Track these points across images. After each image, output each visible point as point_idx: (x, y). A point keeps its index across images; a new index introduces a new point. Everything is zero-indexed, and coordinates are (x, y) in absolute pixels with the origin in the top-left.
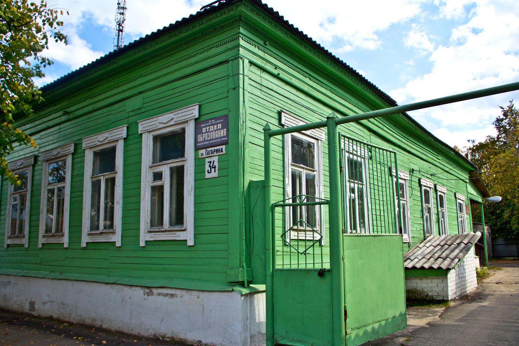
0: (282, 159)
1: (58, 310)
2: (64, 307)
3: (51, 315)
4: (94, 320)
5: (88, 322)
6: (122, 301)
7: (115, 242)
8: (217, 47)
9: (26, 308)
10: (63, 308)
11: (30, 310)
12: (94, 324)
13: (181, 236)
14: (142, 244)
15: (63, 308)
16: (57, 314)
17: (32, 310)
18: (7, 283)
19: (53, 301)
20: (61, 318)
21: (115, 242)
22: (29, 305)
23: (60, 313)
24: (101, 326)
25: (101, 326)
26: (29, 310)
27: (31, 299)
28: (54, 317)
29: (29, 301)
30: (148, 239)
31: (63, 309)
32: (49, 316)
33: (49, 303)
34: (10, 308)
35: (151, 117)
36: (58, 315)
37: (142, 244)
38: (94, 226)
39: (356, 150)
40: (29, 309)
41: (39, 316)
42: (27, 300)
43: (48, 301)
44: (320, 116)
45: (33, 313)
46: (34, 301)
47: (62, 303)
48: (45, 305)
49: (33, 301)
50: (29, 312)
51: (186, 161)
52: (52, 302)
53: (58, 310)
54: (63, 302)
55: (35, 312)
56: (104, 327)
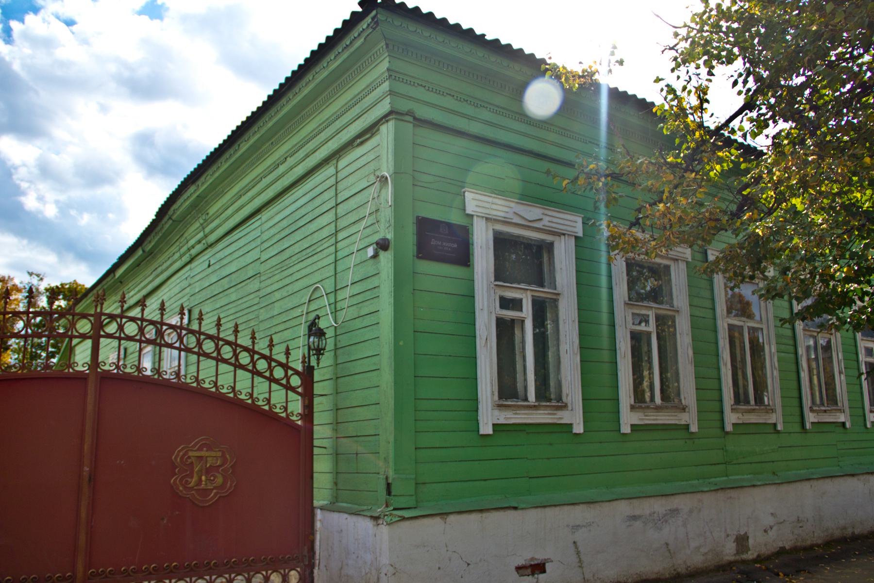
0: (853, 344)
1: (793, 533)
2: (801, 525)
3: (782, 546)
4: (844, 528)
5: (838, 534)
6: (870, 493)
7: (571, 425)
8: (406, 83)
9: (729, 551)
10: (801, 527)
11: (738, 553)
12: (845, 535)
13: (683, 418)
14: (626, 429)
15: (801, 527)
16: (791, 540)
17: (742, 553)
18: (665, 515)
19: (782, 520)
20: (799, 544)
21: (571, 425)
22: (734, 545)
23: (796, 536)
24: (853, 533)
25: (853, 533)
26: (735, 555)
27: (739, 531)
28: (787, 547)
29: (734, 537)
30: (636, 422)
31: (801, 529)
32: (778, 549)
33: (775, 528)
34: (679, 570)
35: (512, 200)
36: (793, 542)
37: (626, 429)
38: (740, 398)
39: (312, 299)
40: (735, 552)
41: (759, 556)
42: (728, 536)
43: (772, 524)
44: (255, 223)
45: (745, 556)
46: (746, 533)
47: (798, 520)
48: (768, 534)
49: (742, 533)
50: (737, 557)
51: (380, 274)
52: (781, 523)
53: (793, 533)
54: (798, 517)
55: (749, 553)
56: (856, 532)
